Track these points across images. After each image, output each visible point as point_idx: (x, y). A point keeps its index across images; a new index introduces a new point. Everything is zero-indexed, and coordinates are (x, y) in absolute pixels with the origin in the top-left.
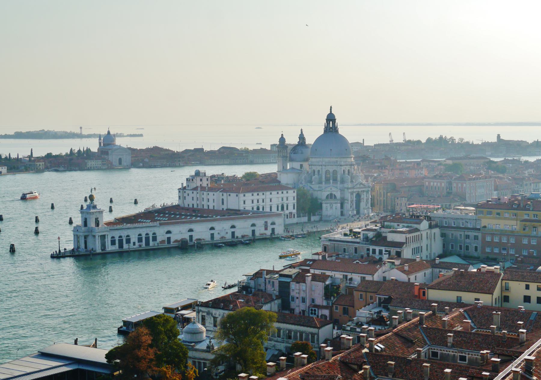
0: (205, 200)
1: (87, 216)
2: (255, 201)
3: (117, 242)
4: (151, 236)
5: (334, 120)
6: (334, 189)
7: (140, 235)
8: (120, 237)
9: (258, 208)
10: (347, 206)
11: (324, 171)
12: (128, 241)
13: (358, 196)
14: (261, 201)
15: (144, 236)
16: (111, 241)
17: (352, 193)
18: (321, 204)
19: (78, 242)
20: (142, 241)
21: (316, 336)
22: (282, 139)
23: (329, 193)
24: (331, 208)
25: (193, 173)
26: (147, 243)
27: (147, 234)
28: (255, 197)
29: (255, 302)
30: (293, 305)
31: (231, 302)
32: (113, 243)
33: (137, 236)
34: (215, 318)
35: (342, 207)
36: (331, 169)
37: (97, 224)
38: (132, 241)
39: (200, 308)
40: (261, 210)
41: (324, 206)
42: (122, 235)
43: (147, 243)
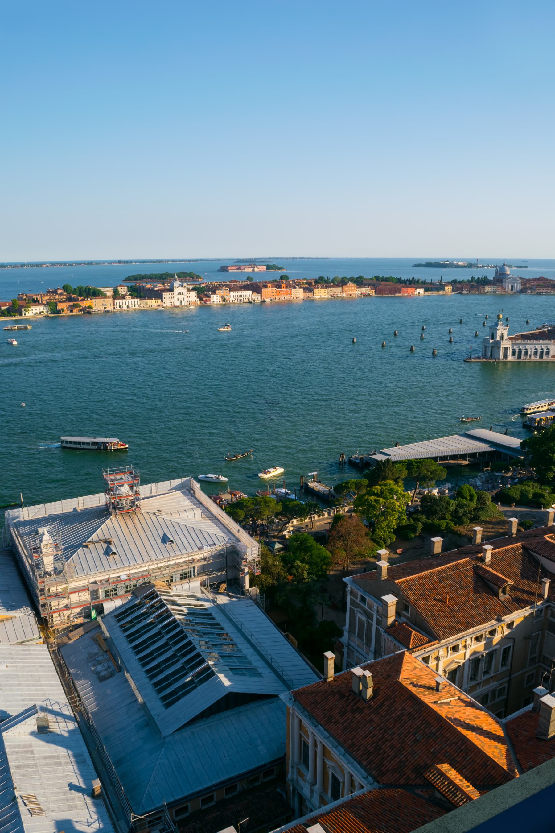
1: (494, 332)
3: (517, 353)
4: (545, 350)
7: (536, 349)
12: (526, 353)
15: (539, 350)
16: (512, 352)
19: (485, 351)
20: (537, 355)
26: (541, 357)
27: (542, 349)
32: (514, 354)
33: (533, 350)
38: (529, 353)
42: (521, 347)
43: (541, 357)
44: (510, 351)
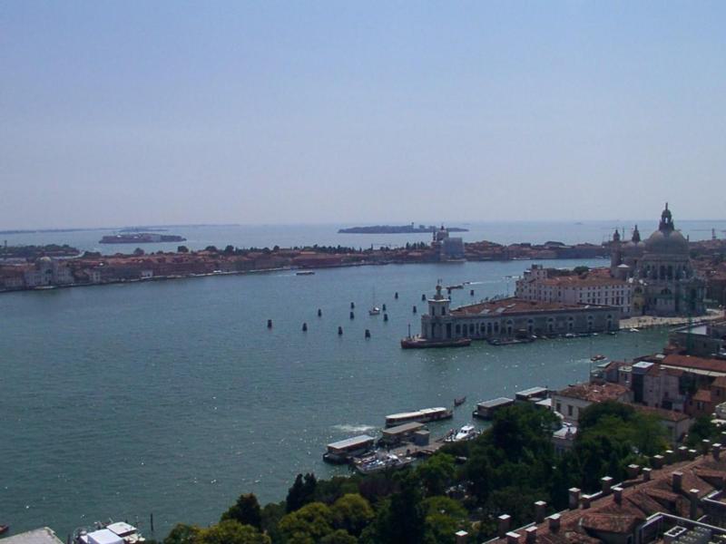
0: (542, 293)
2: (591, 295)
5: (670, 217)
6: (669, 284)
8: (483, 324)
9: (594, 301)
10: (682, 303)
11: (659, 266)
13: (694, 293)
14: (596, 295)
15: (486, 324)
17: (687, 288)
18: (656, 300)
21: (674, 430)
22: (617, 235)
23: (663, 288)
24: (666, 303)
25: (530, 267)
28: (591, 291)
29: (610, 394)
30: (645, 400)
31: (585, 392)
34: (570, 408)
35: (677, 302)
36: (666, 264)
37: (444, 313)
39: (557, 398)
40: (596, 303)
41: (658, 300)
44: (453, 329)
